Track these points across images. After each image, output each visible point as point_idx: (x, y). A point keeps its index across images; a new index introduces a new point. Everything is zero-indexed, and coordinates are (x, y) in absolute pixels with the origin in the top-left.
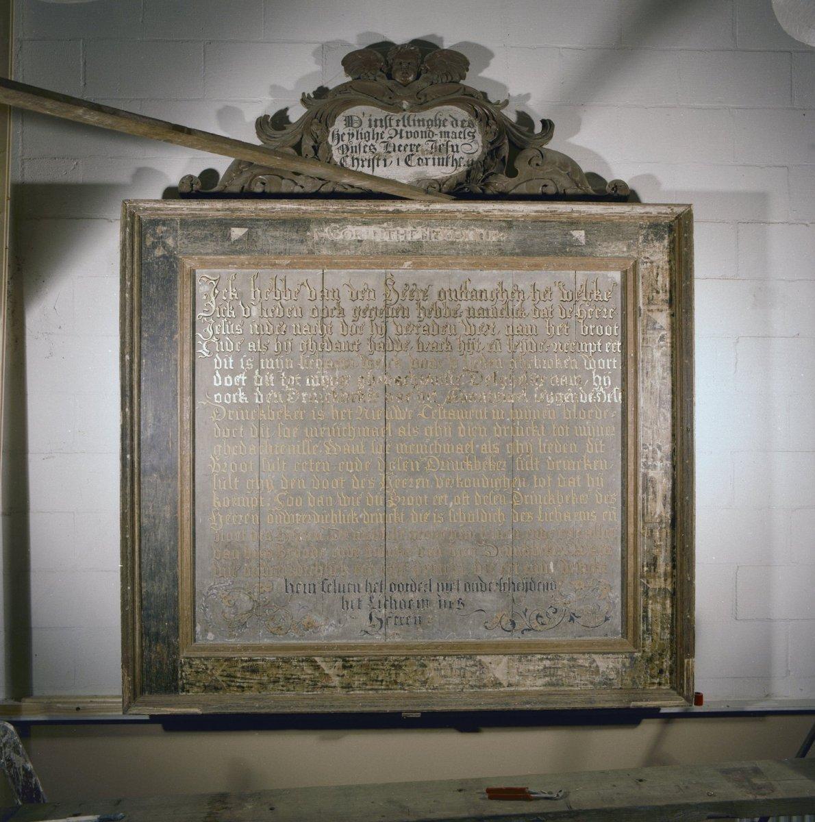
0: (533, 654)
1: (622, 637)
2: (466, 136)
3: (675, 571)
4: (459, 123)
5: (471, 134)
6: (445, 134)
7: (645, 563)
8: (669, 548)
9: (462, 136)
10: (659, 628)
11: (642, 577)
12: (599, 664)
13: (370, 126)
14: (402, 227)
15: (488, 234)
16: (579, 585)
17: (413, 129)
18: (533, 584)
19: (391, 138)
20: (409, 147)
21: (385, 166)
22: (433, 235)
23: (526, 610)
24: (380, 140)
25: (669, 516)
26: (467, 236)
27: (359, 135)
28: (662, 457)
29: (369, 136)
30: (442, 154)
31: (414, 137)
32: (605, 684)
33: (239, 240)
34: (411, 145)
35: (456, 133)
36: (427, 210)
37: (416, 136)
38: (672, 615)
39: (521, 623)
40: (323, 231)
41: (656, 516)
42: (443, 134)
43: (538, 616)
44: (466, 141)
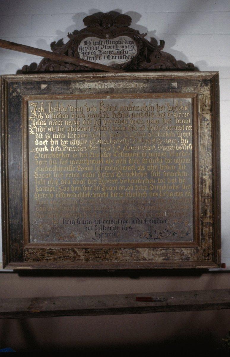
0: (158, 248)
1: (193, 241)
3: (214, 215)
4: (128, 42)
5: (132, 47)
7: (202, 212)
8: (211, 207)
9: (129, 47)
10: (208, 238)
11: (201, 218)
12: (184, 252)
13: (94, 44)
14: (106, 83)
15: (139, 85)
16: (176, 221)
21: (100, 59)
22: (118, 86)
23: (156, 231)
24: (98, 50)
25: (211, 194)
26: (131, 86)
27: (90, 48)
28: (208, 171)
30: (121, 54)
32: (186, 259)
33: (44, 89)
38: (213, 232)
39: (154, 236)
40: (76, 85)
41: (206, 194)
43: (160, 233)
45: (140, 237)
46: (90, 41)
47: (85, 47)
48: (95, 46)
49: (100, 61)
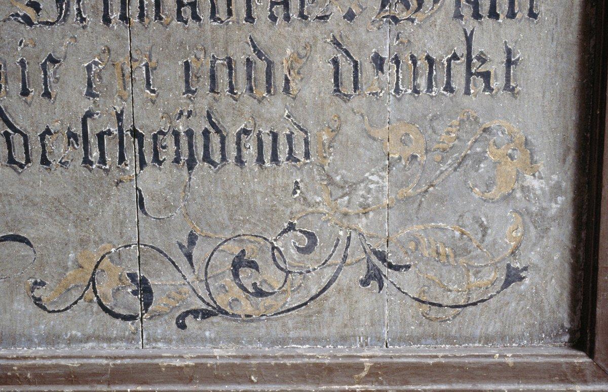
18: (215, 139)
43: (239, 263)
45: (38, 302)
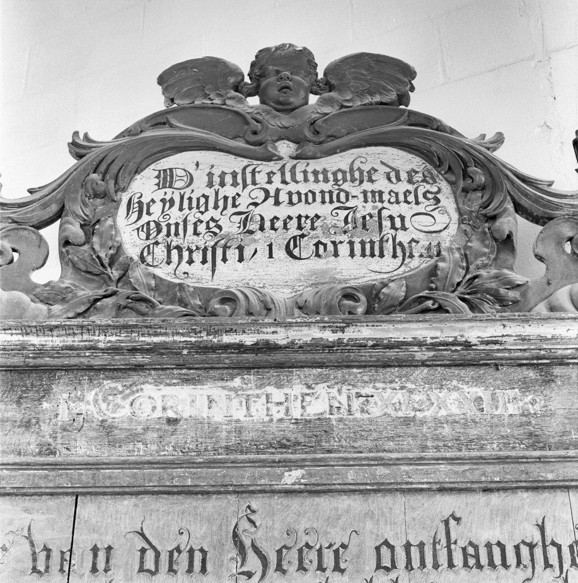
2: (421, 198)
4: (404, 176)
6: (373, 196)
9: (411, 198)
13: (210, 185)
14: (279, 386)
17: (303, 188)
19: (256, 204)
20: (295, 221)
21: (241, 259)
22: (356, 404)
24: (230, 210)
29: (207, 203)
31: (307, 202)
34: (299, 217)
35: (397, 194)
36: (339, 342)
37: (310, 199)
42: (369, 195)
44: (420, 209)
46: (191, 169)
47: (159, 195)
48: (217, 193)
49: (240, 266)
